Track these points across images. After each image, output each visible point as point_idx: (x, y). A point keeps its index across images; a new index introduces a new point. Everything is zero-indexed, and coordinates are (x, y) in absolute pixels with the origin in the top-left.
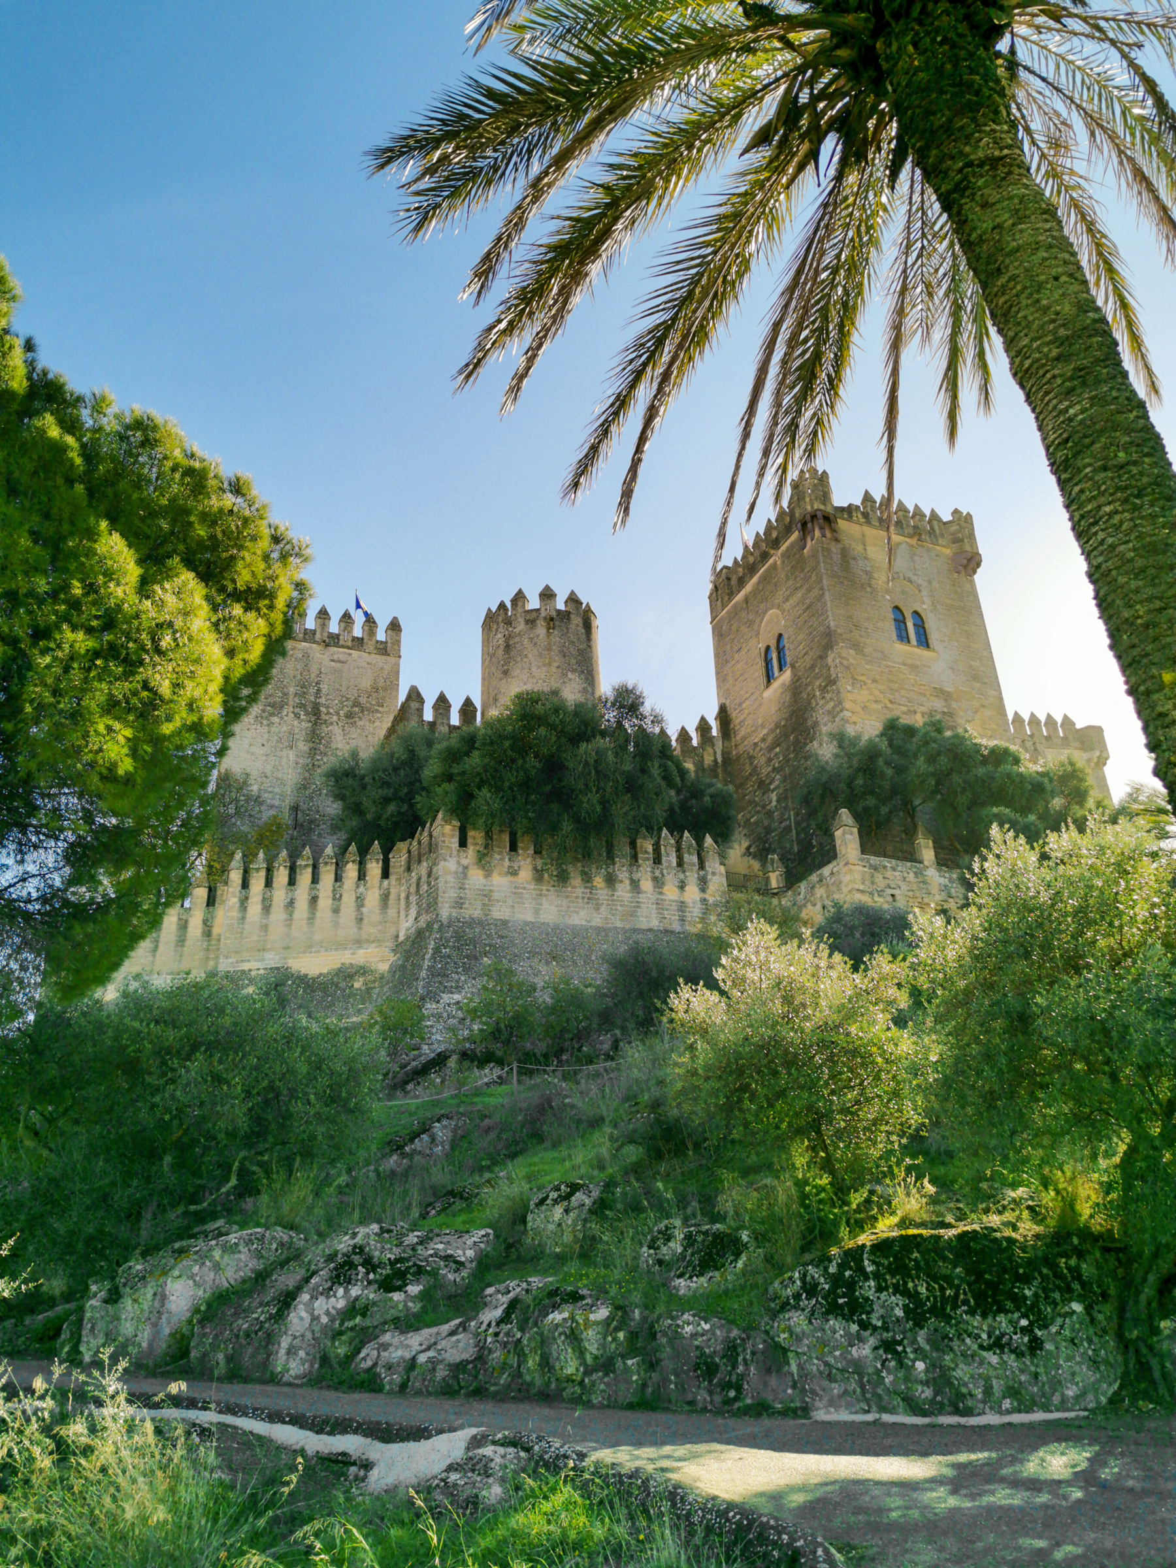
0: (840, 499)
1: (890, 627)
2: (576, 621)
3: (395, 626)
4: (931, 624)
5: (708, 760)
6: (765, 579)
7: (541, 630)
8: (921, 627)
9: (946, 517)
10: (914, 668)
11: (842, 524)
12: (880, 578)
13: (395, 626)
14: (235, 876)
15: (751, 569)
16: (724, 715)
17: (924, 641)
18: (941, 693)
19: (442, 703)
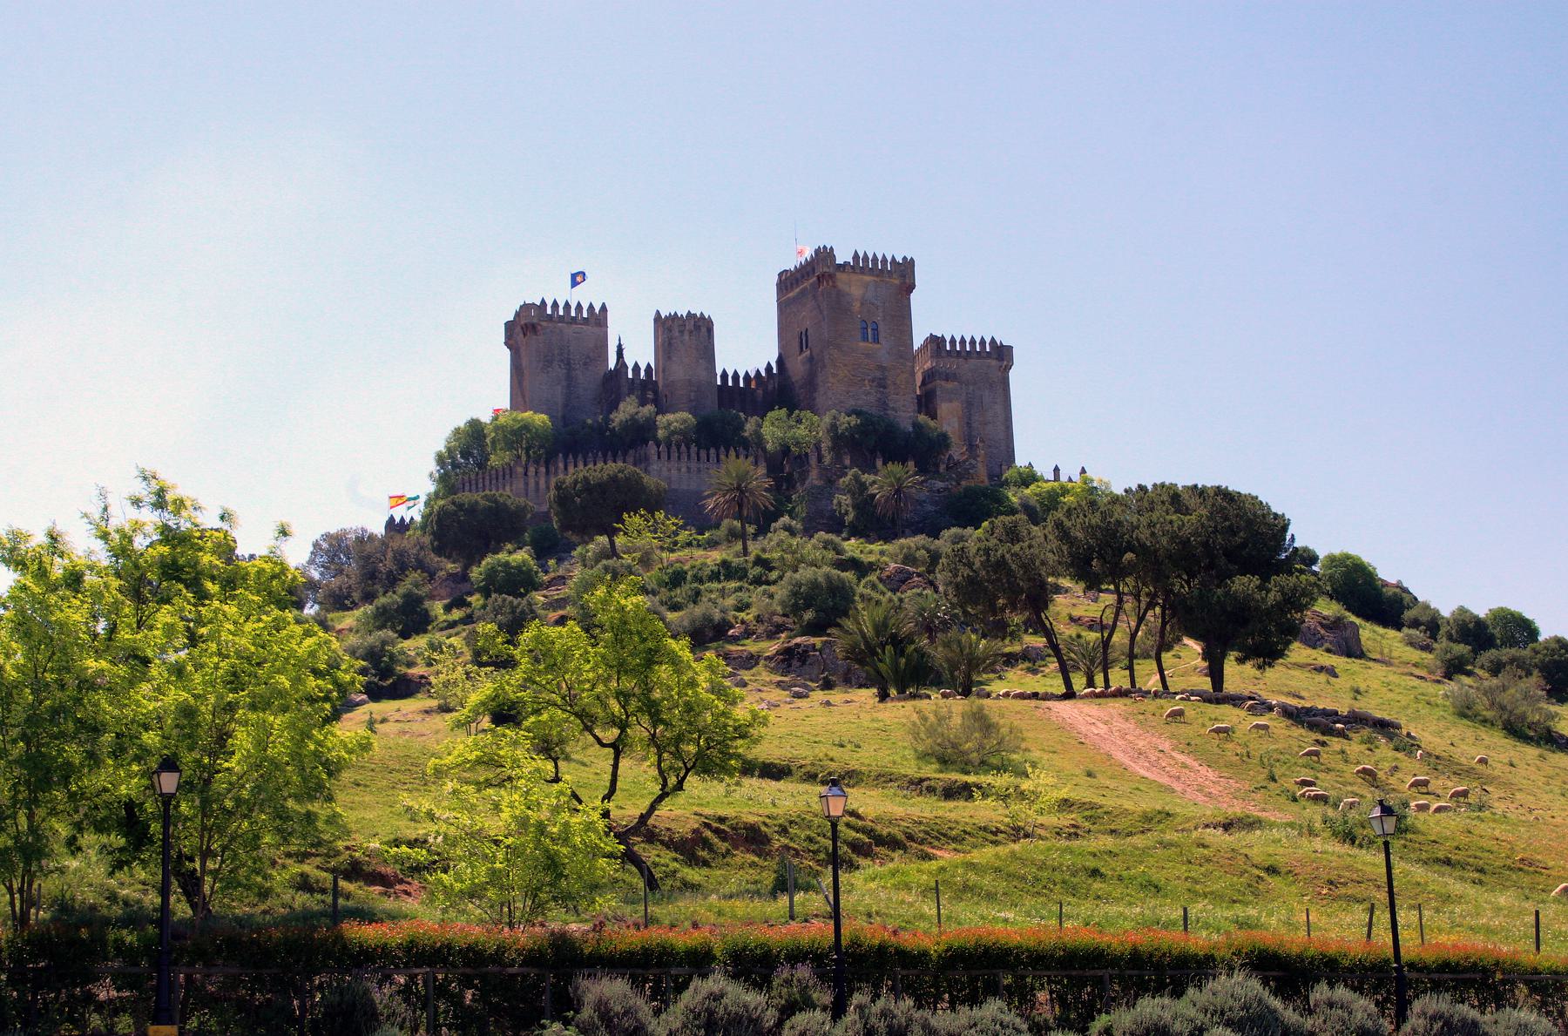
0: (839, 261)
1: (859, 336)
2: (704, 330)
3: (604, 308)
4: (881, 328)
5: (770, 387)
6: (803, 292)
7: (686, 337)
8: (876, 330)
9: (899, 259)
10: (868, 356)
11: (839, 275)
12: (857, 305)
13: (604, 308)
14: (561, 465)
15: (797, 282)
16: (780, 361)
17: (876, 340)
18: (881, 368)
19: (636, 368)
